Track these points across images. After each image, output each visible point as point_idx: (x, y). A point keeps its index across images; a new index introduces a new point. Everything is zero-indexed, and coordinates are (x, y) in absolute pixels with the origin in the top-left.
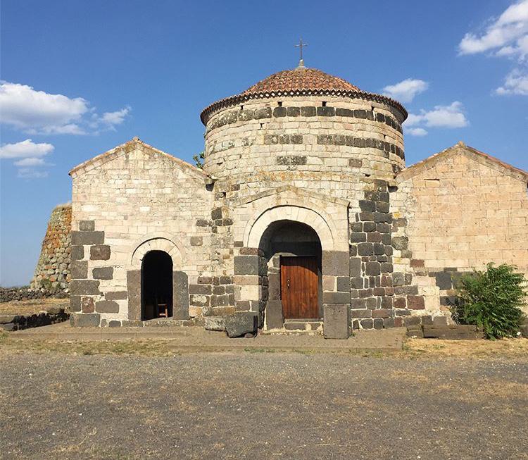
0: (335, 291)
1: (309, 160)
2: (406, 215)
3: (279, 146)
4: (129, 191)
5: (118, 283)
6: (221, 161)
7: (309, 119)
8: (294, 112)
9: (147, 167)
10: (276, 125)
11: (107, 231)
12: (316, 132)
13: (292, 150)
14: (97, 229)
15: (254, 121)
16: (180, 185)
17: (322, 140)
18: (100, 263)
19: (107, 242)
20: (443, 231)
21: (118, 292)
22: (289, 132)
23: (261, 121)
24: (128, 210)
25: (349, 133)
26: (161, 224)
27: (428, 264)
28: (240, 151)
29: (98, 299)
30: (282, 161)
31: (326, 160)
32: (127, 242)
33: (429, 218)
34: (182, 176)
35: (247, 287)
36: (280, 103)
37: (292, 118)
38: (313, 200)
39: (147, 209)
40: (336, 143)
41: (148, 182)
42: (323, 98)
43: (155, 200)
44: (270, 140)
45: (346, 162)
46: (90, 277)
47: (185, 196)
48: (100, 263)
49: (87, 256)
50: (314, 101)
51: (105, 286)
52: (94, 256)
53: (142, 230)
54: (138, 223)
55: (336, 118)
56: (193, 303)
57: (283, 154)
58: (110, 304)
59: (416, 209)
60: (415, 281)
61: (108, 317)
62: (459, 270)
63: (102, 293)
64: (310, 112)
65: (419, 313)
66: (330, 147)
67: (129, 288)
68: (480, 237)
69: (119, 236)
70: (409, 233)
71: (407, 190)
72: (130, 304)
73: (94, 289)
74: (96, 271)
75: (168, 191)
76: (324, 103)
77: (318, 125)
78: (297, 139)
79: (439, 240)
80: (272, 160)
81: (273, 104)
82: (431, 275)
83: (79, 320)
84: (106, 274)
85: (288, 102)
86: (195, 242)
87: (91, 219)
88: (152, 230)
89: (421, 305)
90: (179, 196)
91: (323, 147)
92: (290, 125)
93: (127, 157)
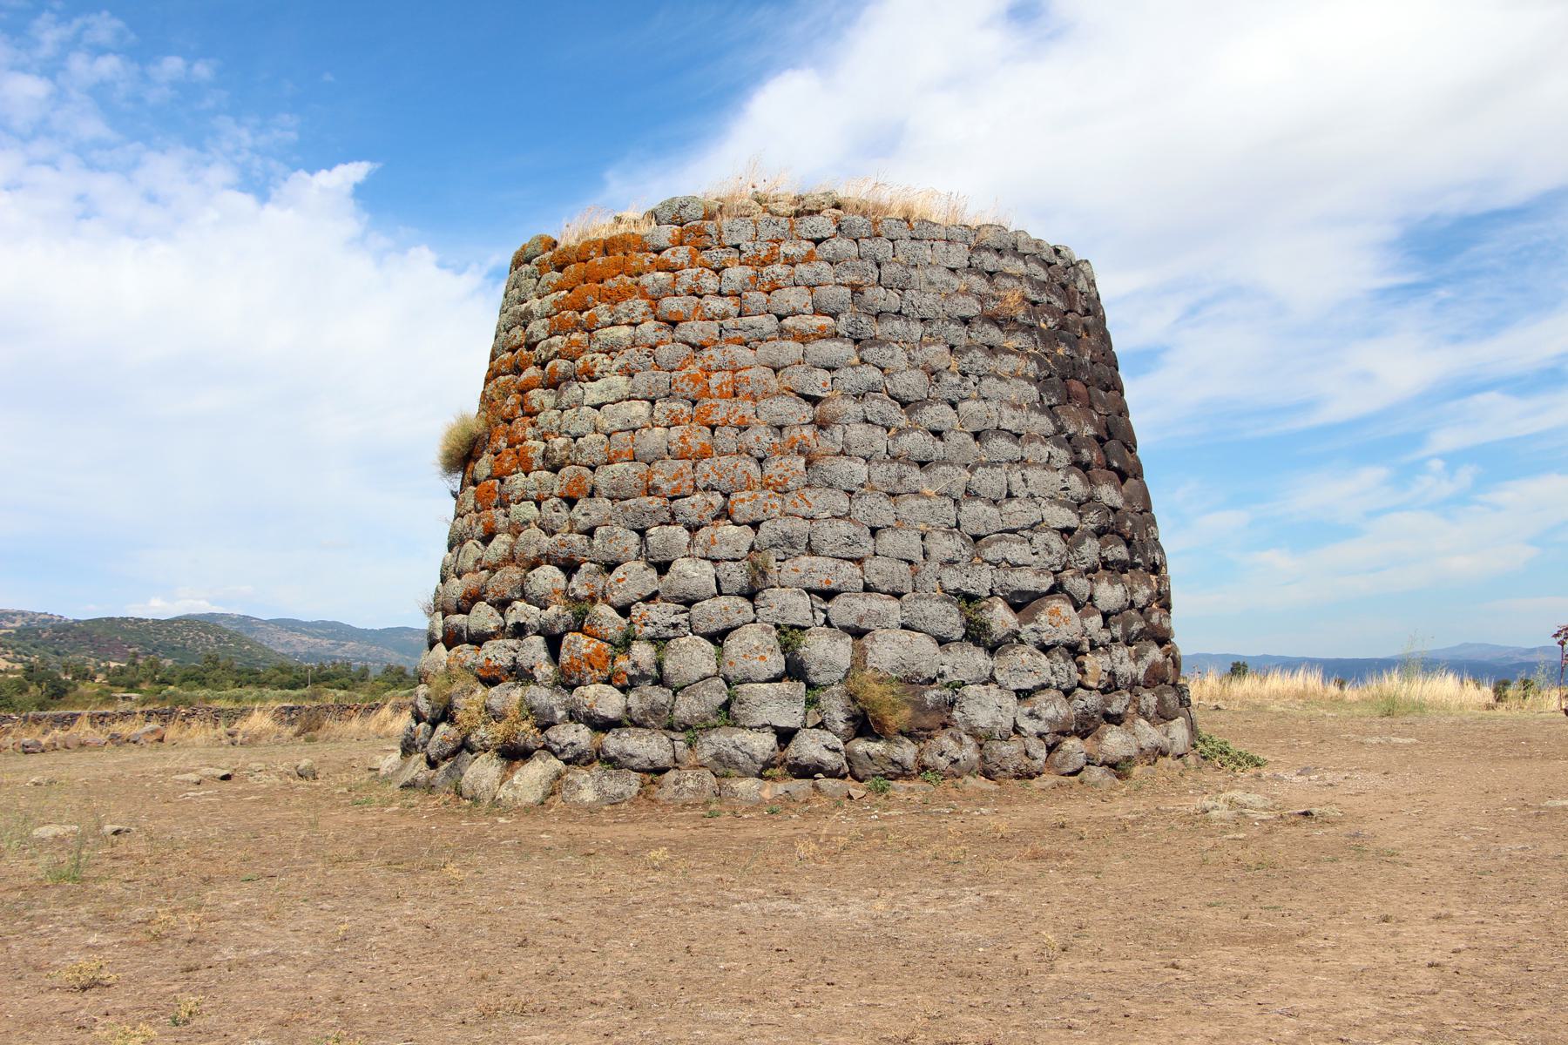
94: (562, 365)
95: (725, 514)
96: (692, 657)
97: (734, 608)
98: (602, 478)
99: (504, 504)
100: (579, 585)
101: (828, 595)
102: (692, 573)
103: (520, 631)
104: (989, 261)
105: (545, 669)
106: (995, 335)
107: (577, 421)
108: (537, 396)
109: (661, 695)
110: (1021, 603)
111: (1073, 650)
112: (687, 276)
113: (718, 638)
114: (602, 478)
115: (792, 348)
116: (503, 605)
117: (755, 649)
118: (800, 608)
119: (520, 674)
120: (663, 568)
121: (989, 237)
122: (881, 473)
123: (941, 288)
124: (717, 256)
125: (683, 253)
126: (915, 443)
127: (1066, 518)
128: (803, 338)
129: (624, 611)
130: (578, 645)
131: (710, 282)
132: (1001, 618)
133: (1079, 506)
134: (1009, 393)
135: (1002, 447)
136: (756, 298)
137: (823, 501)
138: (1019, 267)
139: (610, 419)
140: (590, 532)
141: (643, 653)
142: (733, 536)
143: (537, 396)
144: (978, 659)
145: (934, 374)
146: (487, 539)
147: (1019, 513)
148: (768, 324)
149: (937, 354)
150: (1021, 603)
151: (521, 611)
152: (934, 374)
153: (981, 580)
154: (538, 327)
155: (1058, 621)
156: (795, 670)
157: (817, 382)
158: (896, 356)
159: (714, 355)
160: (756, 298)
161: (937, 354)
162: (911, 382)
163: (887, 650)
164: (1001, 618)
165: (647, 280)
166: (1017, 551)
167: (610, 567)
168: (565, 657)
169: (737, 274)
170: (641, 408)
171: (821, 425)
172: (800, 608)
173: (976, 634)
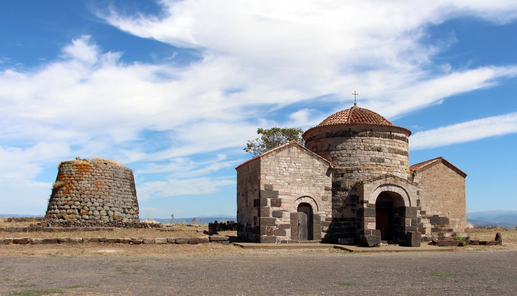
1: (386, 160)
4: (290, 169)
5: (286, 219)
9: (300, 157)
10: (370, 141)
11: (280, 191)
12: (388, 146)
13: (378, 155)
14: (274, 189)
16: (316, 168)
17: (391, 150)
18: (276, 209)
19: (280, 197)
20: (433, 198)
22: (376, 145)
23: (362, 138)
25: (399, 148)
26: (307, 189)
27: (427, 213)
28: (350, 152)
29: (275, 228)
30: (372, 160)
31: (393, 161)
32: (289, 198)
33: (428, 191)
34: (318, 163)
35: (370, 223)
37: (377, 138)
38: (402, 182)
39: (300, 180)
40: (396, 153)
41: (301, 165)
43: (304, 175)
45: (399, 162)
47: (319, 174)
49: (269, 204)
51: (278, 221)
52: (273, 204)
54: (296, 187)
55: (395, 140)
57: (373, 156)
60: (422, 221)
61: (281, 238)
62: (439, 216)
63: (277, 225)
65: (423, 236)
66: (394, 154)
67: (291, 222)
68: (448, 201)
69: (286, 194)
73: (273, 222)
74: (274, 213)
75: (310, 171)
78: (379, 150)
79: (432, 202)
82: (428, 218)
83: (265, 240)
84: (278, 215)
86: (324, 199)
87: (271, 183)
88: (303, 191)
89: (424, 233)
90: (316, 173)
91: (391, 155)
93: (289, 150)
94: (78, 178)
95: (100, 198)
96: (97, 213)
97: (100, 208)
98: (85, 192)
99: (69, 193)
100: (83, 204)
101: (111, 207)
102: (97, 204)
103: (74, 209)
104: (126, 172)
105: (78, 213)
106: (126, 180)
107: (82, 185)
108: (74, 181)
109: (93, 217)
110: (129, 209)
111: (133, 214)
112: (95, 170)
113: (99, 211)
114: (85, 192)
115: (107, 180)
116: (70, 206)
117: (103, 212)
118: (108, 209)
119: (75, 214)
120: (93, 203)
121: (126, 169)
122: (116, 195)
123: (122, 175)
124: (98, 169)
125: (94, 168)
126: (119, 192)
127: (132, 200)
128: (108, 179)
129: (88, 207)
130: (82, 211)
131: (98, 172)
132: (127, 211)
133: (133, 199)
134: (127, 187)
135: (127, 192)
136: (103, 174)
137: (110, 197)
138: (128, 172)
139: (86, 186)
140: (84, 198)
141: (91, 212)
142: (101, 200)
143: (74, 181)
144: (125, 215)
145: (121, 184)
146: (67, 197)
147: (128, 200)
148: (104, 177)
149: (121, 182)
150: (129, 209)
151: (73, 207)
152: (121, 184)
153: (125, 207)
154: (74, 173)
155: (132, 211)
156: (108, 215)
157: (110, 184)
158: (117, 182)
159: (98, 180)
160: (103, 174)
161: (121, 182)
162: (119, 185)
163: (117, 213)
164: (127, 211)
165: (90, 170)
166: (128, 204)
167: (87, 203)
168: (81, 212)
169: (101, 171)
170: (90, 185)
171: (110, 189)
172: (108, 209)
173: (125, 212)
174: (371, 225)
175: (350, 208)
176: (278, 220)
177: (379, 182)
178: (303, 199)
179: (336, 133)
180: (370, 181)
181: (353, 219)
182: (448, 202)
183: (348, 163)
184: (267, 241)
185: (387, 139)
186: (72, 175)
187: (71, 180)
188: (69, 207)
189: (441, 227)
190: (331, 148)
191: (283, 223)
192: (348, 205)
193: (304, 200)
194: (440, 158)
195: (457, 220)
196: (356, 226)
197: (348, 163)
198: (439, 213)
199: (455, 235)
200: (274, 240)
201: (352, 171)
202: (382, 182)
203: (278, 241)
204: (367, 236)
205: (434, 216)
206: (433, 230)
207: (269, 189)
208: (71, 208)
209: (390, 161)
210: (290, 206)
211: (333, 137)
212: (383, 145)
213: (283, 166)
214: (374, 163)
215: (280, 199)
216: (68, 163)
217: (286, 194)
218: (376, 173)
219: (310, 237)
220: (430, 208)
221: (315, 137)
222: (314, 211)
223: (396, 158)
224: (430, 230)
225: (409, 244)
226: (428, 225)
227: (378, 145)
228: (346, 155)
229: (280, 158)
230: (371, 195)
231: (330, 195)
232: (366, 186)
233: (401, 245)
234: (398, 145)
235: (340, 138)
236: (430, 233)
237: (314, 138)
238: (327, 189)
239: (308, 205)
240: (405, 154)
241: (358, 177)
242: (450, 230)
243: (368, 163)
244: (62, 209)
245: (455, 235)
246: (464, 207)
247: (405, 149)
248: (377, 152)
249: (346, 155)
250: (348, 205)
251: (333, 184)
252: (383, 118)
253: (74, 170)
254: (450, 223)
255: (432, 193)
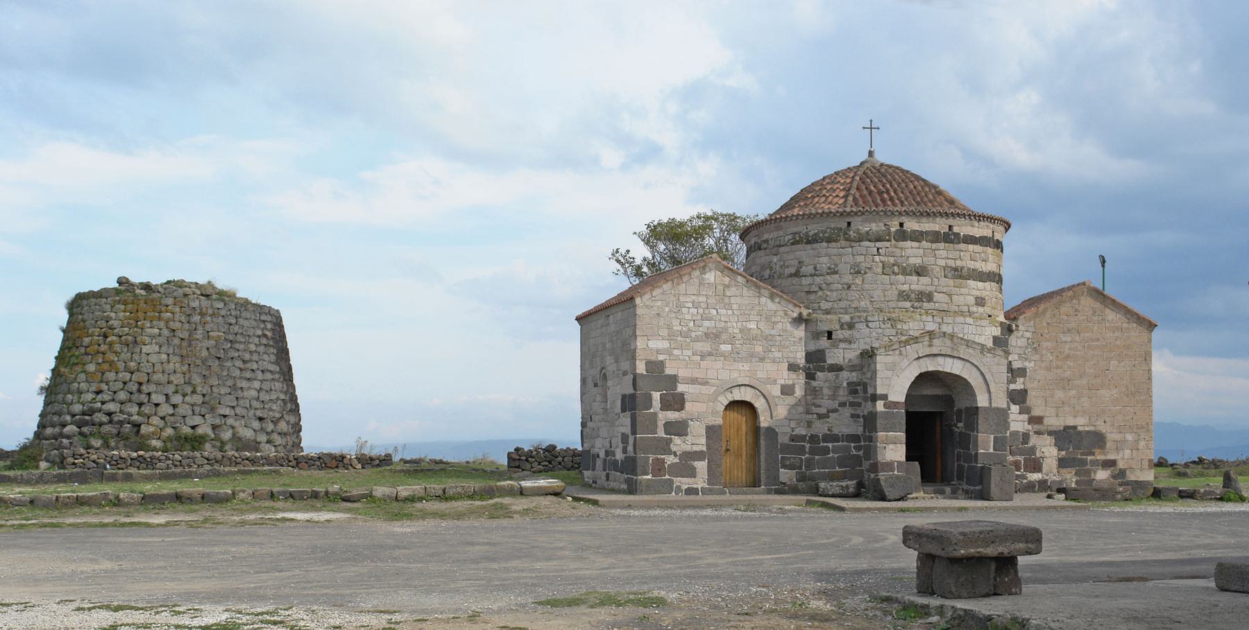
0: (991, 450)
1: (937, 297)
2: (1027, 364)
3: (900, 277)
5: (696, 440)
6: (814, 288)
7: (934, 246)
8: (917, 236)
9: (728, 293)
10: (898, 252)
11: (682, 373)
12: (942, 263)
14: (668, 371)
15: (867, 243)
18: (673, 416)
19: (681, 388)
20: (1064, 383)
21: (696, 452)
22: (912, 261)
23: (878, 244)
24: (705, 347)
25: (972, 265)
27: (1046, 421)
28: (848, 278)
29: (670, 460)
30: (903, 296)
31: (954, 297)
35: (891, 446)
36: (901, 225)
37: (915, 244)
38: (971, 351)
39: (728, 347)
40: (961, 277)
42: (951, 221)
44: (887, 269)
45: (971, 300)
46: (661, 433)
48: (673, 416)
50: (939, 225)
51: (678, 444)
52: (666, 406)
53: (724, 375)
55: (962, 246)
56: (784, 467)
57: (906, 287)
58: (685, 466)
59: (1037, 357)
61: (684, 482)
62: (1080, 428)
64: (936, 237)
65: (1035, 477)
67: (708, 445)
69: (694, 381)
70: (1029, 386)
71: (1028, 335)
72: (709, 467)
73: (665, 447)
74: (669, 426)
75: (752, 325)
76: (950, 227)
77: (943, 253)
78: (920, 271)
79: (1060, 394)
80: (892, 294)
81: (894, 228)
82: (1050, 433)
84: (679, 428)
85: (911, 225)
87: (661, 358)
91: (951, 282)
92: (913, 253)
100: (147, 409)
126: (248, 375)
127: (282, 396)
133: (286, 393)
139: (153, 358)
140: (149, 394)
143: (117, 347)
146: (99, 392)
154: (115, 323)
174: (893, 449)
175: (847, 411)
176: (677, 440)
177: (911, 350)
178: (736, 391)
179: (815, 234)
180: (888, 348)
181: (854, 438)
182: (1105, 394)
183: (843, 304)
184: (650, 488)
185: (942, 245)
186: (111, 328)
187: (111, 344)
188: (105, 419)
189: (1082, 454)
190: (803, 269)
191: (688, 448)
192: (842, 405)
193: (738, 395)
194: (1084, 284)
195: (1129, 437)
196: (861, 453)
197: (843, 304)
198: (1082, 423)
199: (1122, 473)
200: (668, 487)
201: (851, 326)
202: (922, 349)
203: (679, 489)
204: (882, 476)
205: (1066, 428)
206: (1062, 463)
207: (655, 367)
208: (111, 422)
209: (946, 299)
210: (704, 409)
211: (808, 242)
212: (929, 260)
213: (688, 317)
214: (908, 304)
215: (682, 395)
216: (92, 295)
217: (694, 381)
218: (913, 327)
219: (755, 483)
220: (1053, 410)
221: (766, 241)
222: (762, 418)
223: (964, 291)
224: (1055, 463)
225: (984, 495)
226: (1049, 452)
227: (918, 261)
228: (840, 286)
229: (682, 299)
230: (895, 382)
231: (799, 381)
232: (881, 360)
233: (969, 495)
234: (970, 257)
235: (825, 244)
236: (1055, 471)
237: (764, 246)
238: (793, 367)
239: (747, 406)
240: (996, 278)
241: (865, 337)
242: (1110, 464)
243: (892, 304)
244: (86, 423)
245: (1122, 473)
246: (1147, 403)
247: (990, 267)
248: (915, 278)
249: (840, 286)
250: (842, 405)
251: (810, 357)
252: (935, 187)
253: (118, 316)
254: (1108, 445)
255: (1059, 371)
